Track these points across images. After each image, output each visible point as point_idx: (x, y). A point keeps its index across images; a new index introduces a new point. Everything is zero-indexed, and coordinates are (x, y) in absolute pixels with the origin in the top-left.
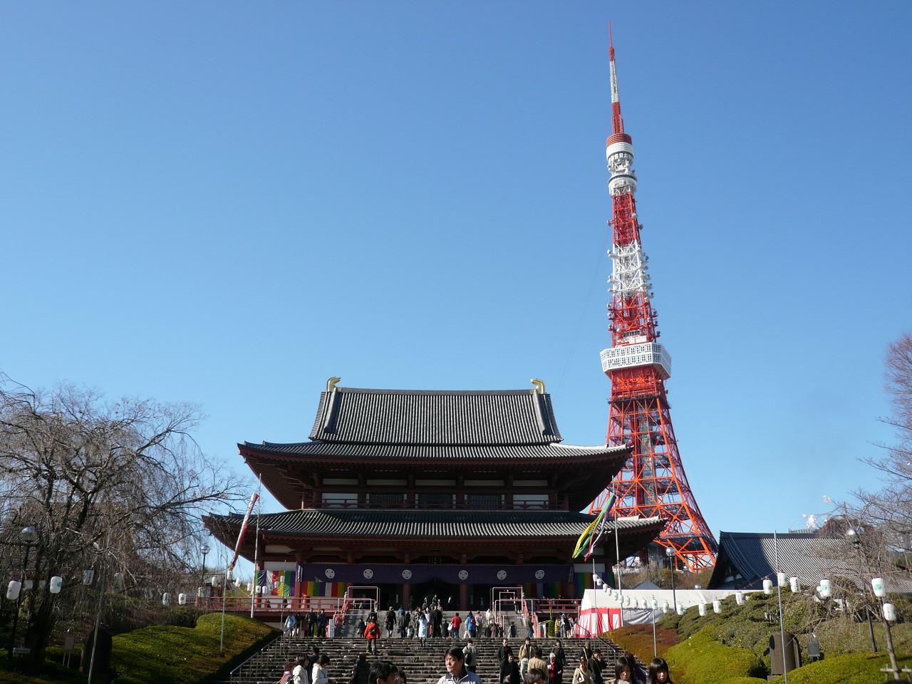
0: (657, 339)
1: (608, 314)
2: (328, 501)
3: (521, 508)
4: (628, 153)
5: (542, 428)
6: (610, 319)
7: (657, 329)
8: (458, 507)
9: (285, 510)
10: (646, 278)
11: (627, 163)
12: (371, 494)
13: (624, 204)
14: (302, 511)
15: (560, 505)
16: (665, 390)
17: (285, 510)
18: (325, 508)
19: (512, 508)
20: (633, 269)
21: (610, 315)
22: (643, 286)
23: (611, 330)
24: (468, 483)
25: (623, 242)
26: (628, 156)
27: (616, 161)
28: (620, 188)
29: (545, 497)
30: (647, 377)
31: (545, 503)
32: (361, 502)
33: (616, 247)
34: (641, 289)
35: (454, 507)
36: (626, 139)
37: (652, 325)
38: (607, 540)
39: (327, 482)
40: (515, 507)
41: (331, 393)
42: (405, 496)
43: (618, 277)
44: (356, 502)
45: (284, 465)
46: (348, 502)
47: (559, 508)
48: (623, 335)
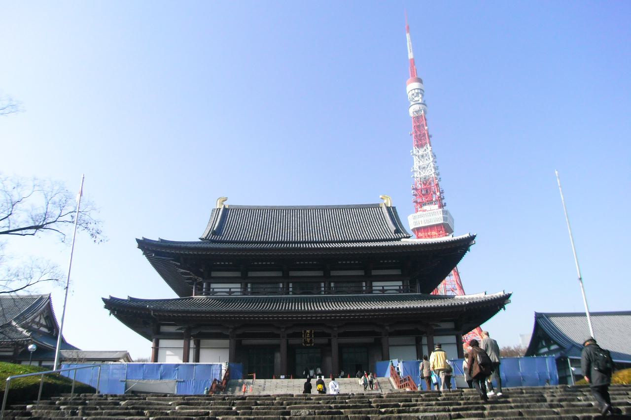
1: (412, 192)
2: (215, 290)
3: (379, 292)
4: (421, 89)
5: (393, 228)
6: (413, 195)
7: (444, 201)
9: (178, 297)
10: (436, 168)
11: (420, 96)
12: (252, 283)
14: (193, 298)
15: (413, 289)
17: (178, 297)
18: (213, 295)
19: (371, 292)
20: (427, 162)
21: (414, 193)
22: (434, 173)
23: (414, 202)
24: (334, 273)
25: (420, 146)
26: (422, 91)
27: (413, 94)
29: (400, 283)
30: (440, 231)
31: (400, 287)
32: (244, 292)
33: (416, 148)
34: (433, 175)
35: (323, 293)
36: (420, 80)
37: (440, 199)
38: (465, 310)
39: (214, 274)
40: (374, 292)
41: (220, 209)
42: (281, 285)
43: (417, 167)
44: (239, 290)
45: (177, 258)
46: (232, 290)
47: (412, 291)
48: (422, 204)
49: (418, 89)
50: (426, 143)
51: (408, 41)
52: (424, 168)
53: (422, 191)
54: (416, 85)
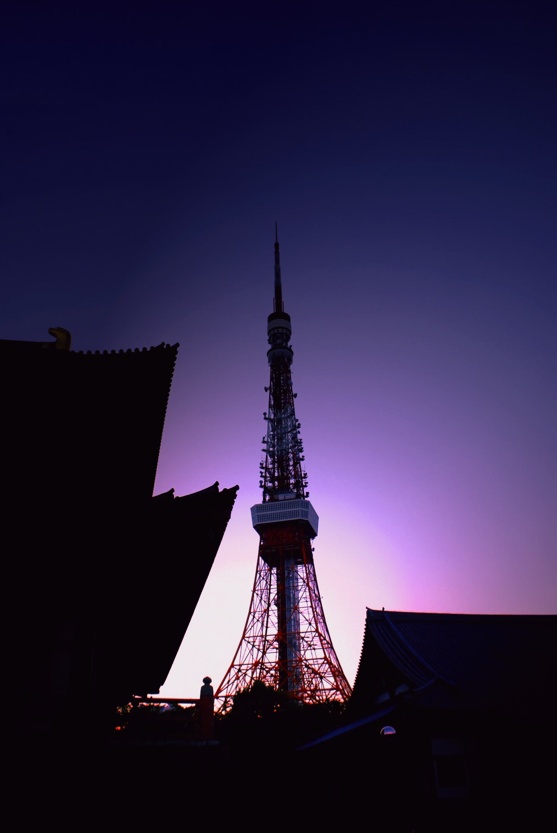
0: (306, 499)
7: (306, 490)
16: (312, 547)
23: (261, 486)
37: (299, 485)
53: (274, 472)
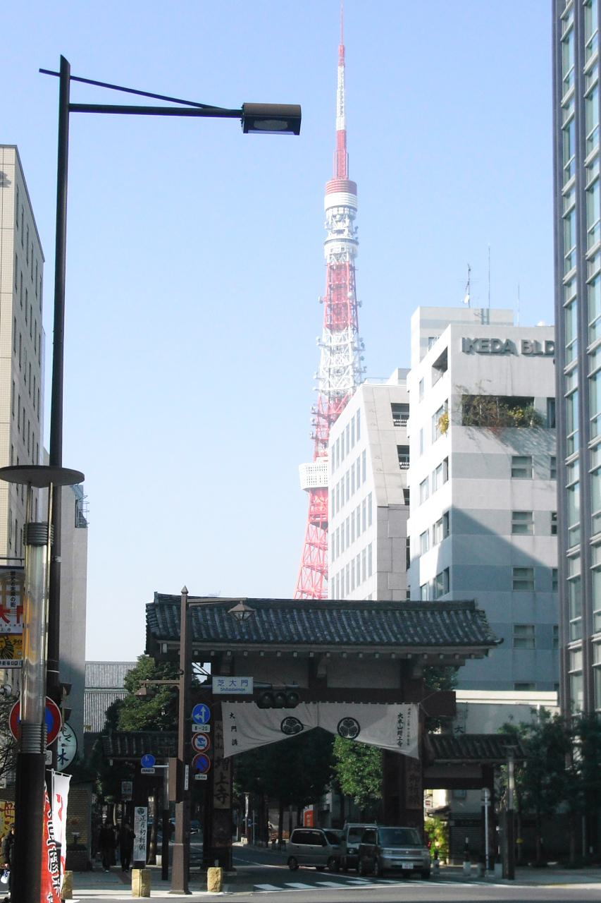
1: (311, 419)
4: (350, 207)
8: (248, 828)
11: (347, 220)
13: (342, 277)
21: (313, 421)
23: (313, 438)
26: (351, 212)
27: (334, 216)
28: (338, 256)
36: (351, 188)
49: (344, 206)
50: (346, 325)
51: (339, 85)
52: (338, 372)
54: (341, 198)
